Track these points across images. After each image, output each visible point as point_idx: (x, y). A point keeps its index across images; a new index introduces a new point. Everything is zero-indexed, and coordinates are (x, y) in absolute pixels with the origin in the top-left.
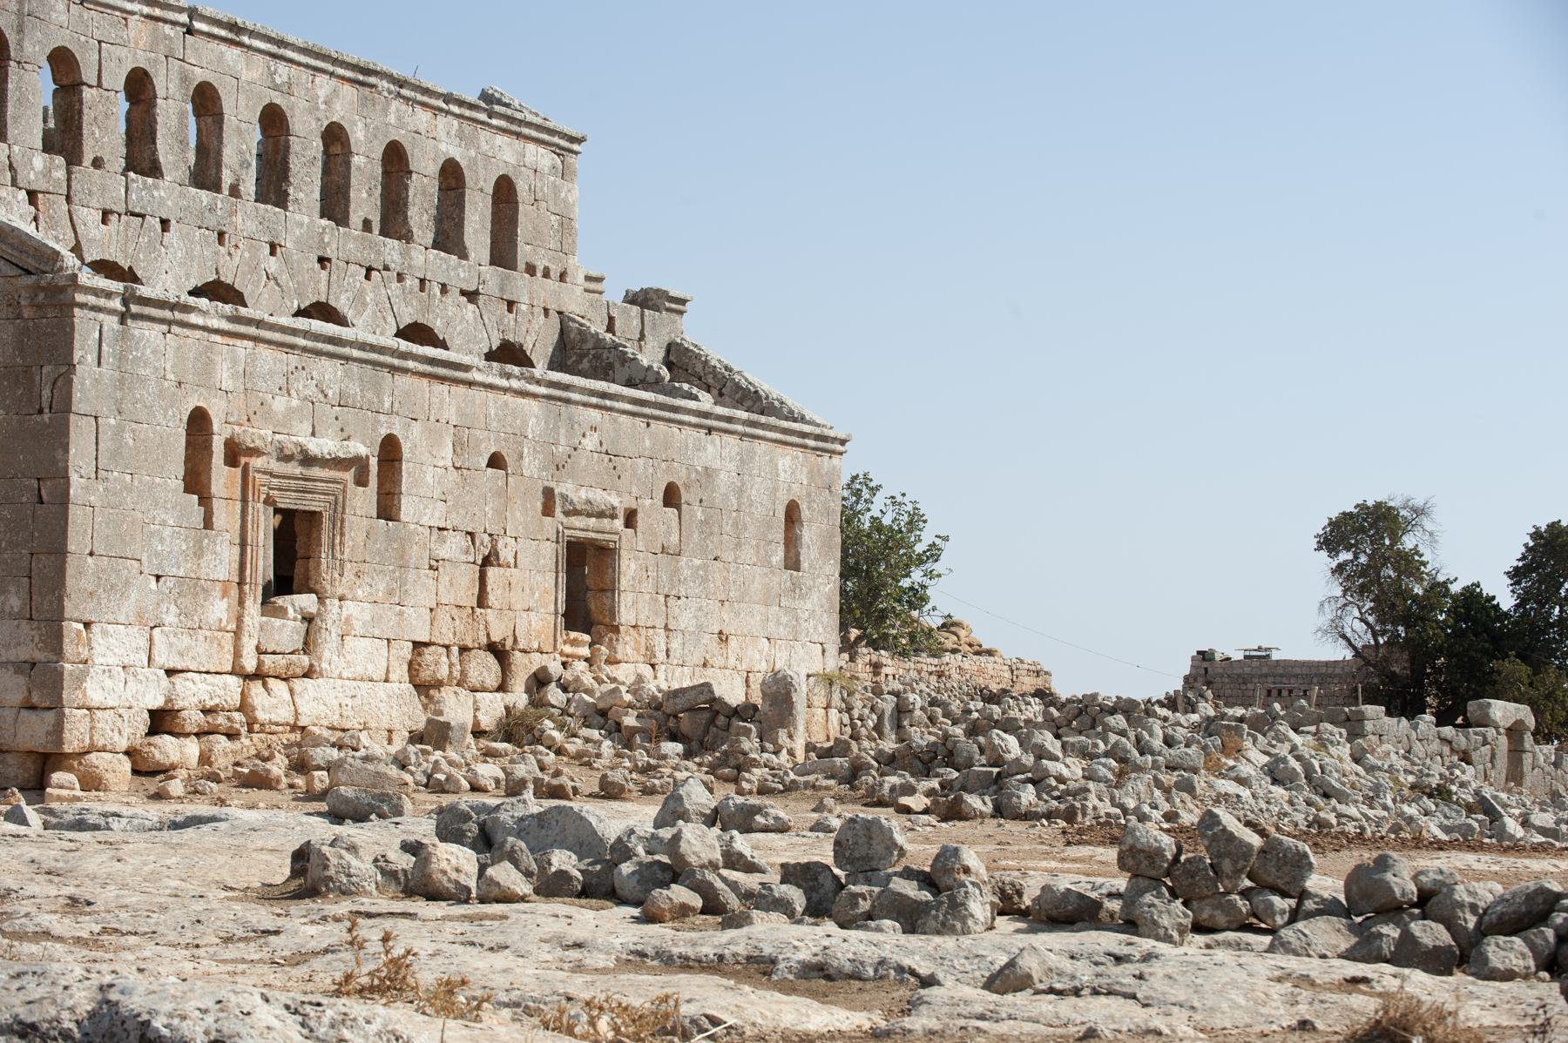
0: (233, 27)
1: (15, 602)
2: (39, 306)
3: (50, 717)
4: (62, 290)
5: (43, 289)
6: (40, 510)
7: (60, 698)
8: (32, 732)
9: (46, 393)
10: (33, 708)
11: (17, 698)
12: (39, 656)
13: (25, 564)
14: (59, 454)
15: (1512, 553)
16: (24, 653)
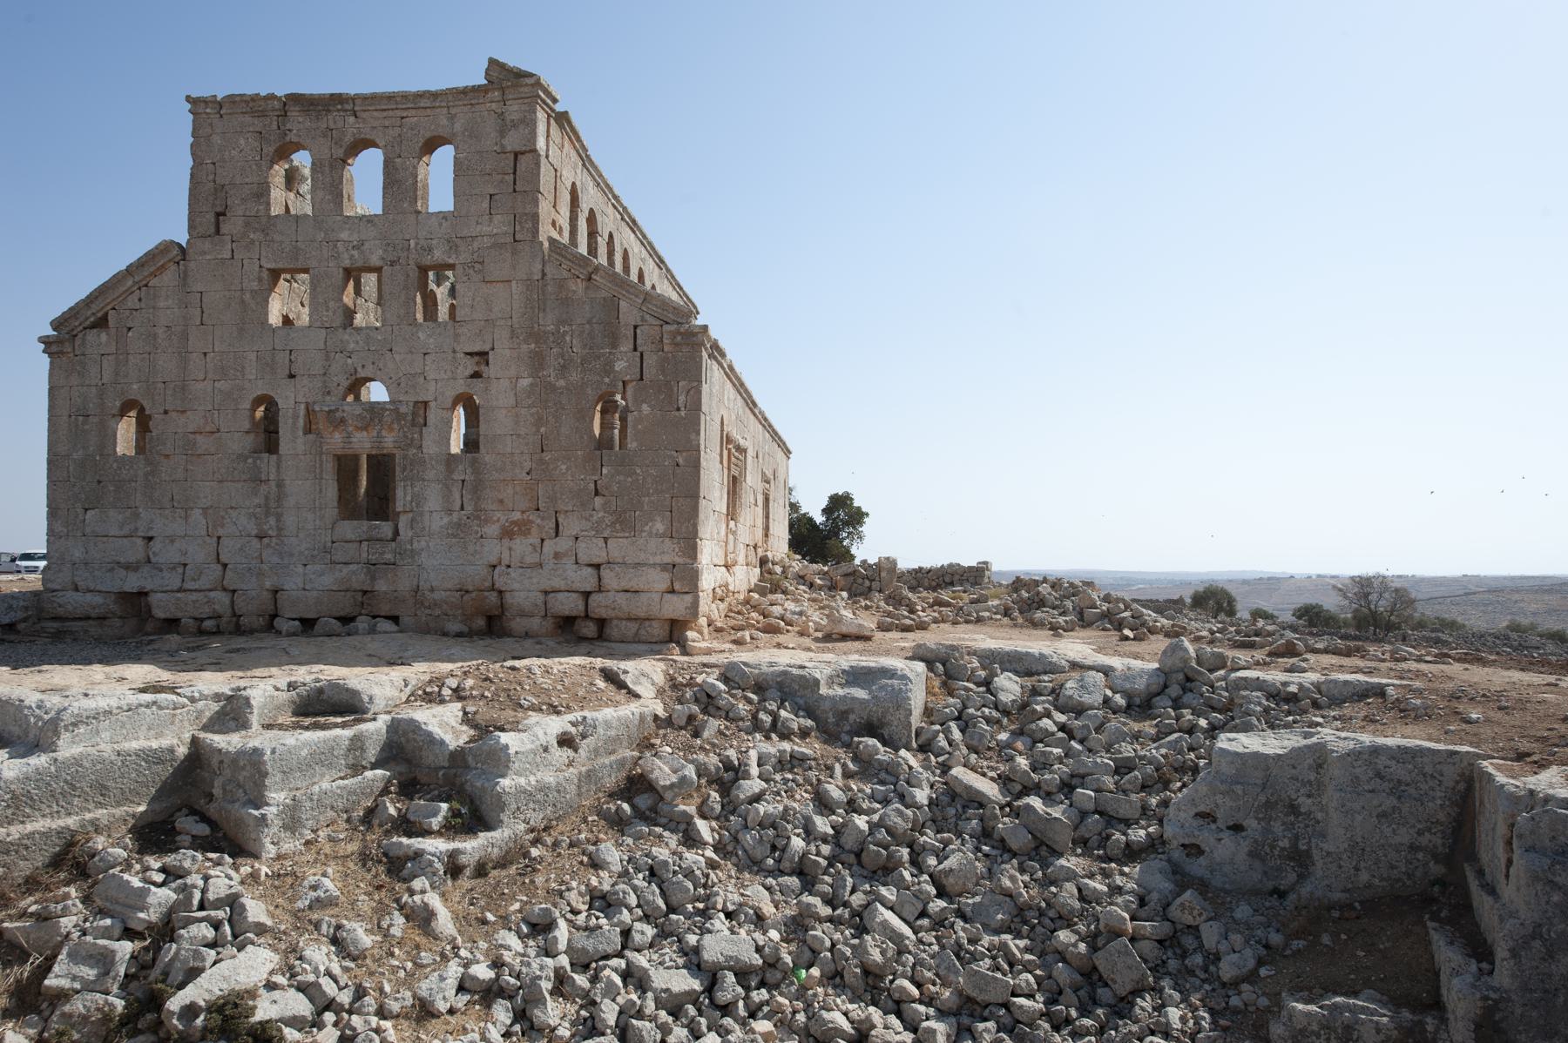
0: (634, 221)
1: (660, 526)
2: (677, 345)
3: (688, 598)
4: (694, 334)
5: (680, 333)
6: (678, 470)
7: (696, 586)
8: (675, 607)
9: (682, 398)
10: (673, 591)
11: (664, 586)
12: (678, 560)
13: (668, 503)
14: (693, 436)
15: (824, 503)
16: (667, 559)
